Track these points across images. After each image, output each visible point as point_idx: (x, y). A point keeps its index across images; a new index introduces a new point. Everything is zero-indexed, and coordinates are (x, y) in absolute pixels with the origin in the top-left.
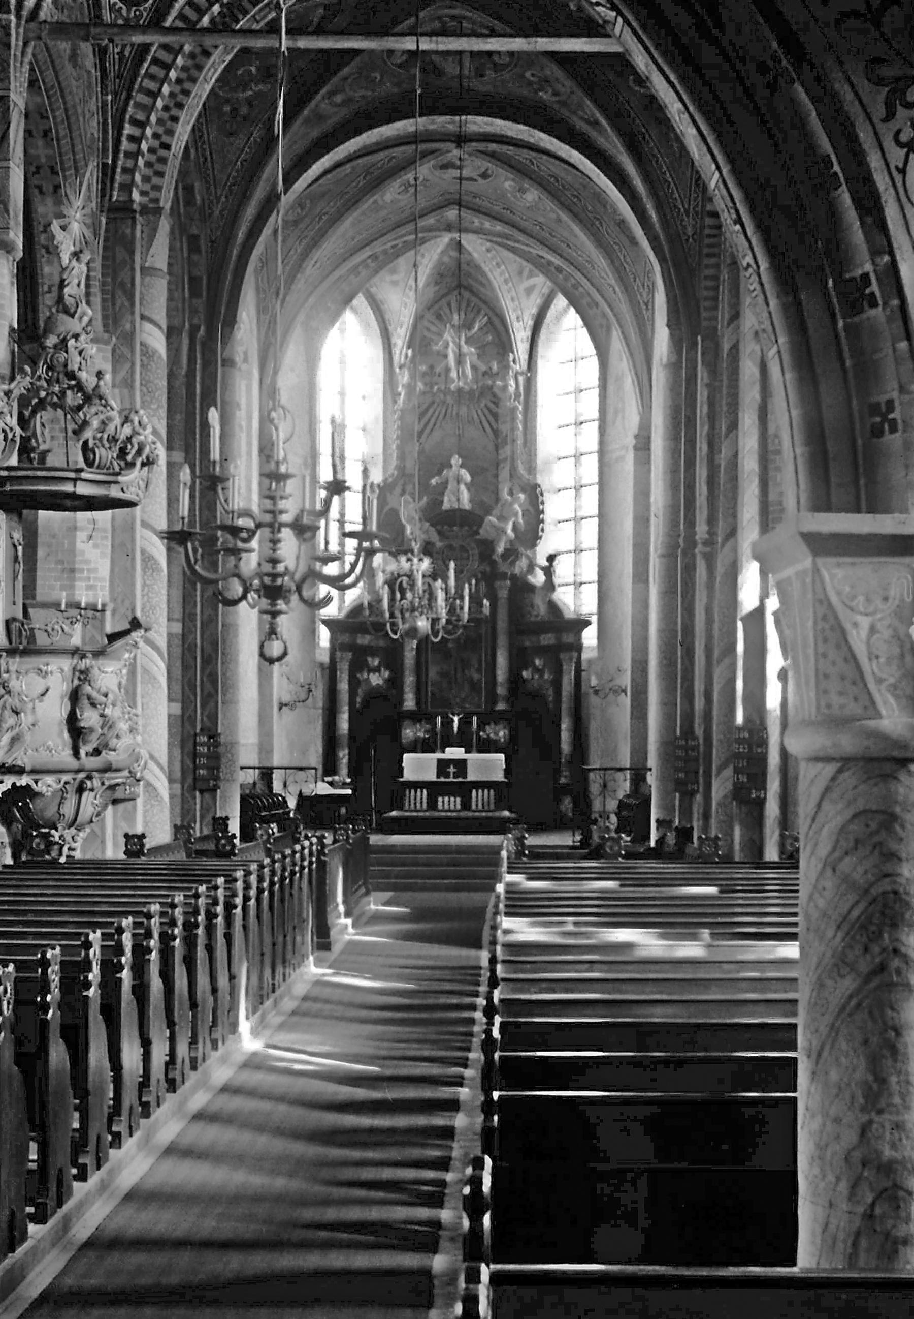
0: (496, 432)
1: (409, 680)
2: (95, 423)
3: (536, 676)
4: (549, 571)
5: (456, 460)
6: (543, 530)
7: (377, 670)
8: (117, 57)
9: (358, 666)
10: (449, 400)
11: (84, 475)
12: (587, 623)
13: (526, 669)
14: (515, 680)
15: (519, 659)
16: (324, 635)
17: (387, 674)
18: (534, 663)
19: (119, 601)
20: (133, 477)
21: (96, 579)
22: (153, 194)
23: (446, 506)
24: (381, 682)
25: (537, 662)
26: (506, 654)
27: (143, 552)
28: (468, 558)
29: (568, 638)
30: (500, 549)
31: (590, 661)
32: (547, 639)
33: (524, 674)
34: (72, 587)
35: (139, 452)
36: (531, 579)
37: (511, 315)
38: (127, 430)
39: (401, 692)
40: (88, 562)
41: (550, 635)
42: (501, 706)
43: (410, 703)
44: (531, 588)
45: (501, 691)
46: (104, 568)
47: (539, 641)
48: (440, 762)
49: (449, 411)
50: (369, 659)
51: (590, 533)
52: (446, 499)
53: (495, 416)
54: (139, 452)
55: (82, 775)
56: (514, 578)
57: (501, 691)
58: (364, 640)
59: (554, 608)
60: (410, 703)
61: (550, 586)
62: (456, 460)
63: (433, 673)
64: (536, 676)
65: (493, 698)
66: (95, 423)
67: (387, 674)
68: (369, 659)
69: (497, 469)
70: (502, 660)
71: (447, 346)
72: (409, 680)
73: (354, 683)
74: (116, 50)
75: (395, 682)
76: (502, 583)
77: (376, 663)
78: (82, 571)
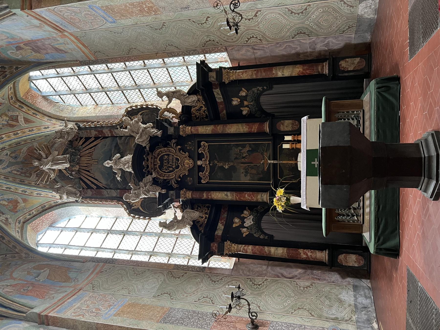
0: (96, 138)
1: (247, 197)
3: (246, 103)
4: (170, 96)
5: (108, 164)
6: (152, 105)
7: (243, 220)
10: (77, 168)
13: (242, 111)
18: (236, 106)
23: (130, 170)
24: (252, 217)
25: (235, 102)
26: (229, 126)
28: (168, 155)
30: (154, 131)
31: (232, 60)
33: (244, 113)
36: (179, 110)
37: (47, 132)
41: (215, 93)
42: (267, 129)
43: (264, 197)
44: (186, 109)
45: (255, 128)
47: (221, 102)
48: (308, 174)
49: (84, 168)
50: (234, 226)
52: (127, 170)
53: (87, 139)
56: (180, 123)
57: (255, 128)
59: (193, 91)
62: (108, 164)
63: (245, 179)
64: (246, 103)
65: (261, 134)
68: (234, 226)
69: (117, 137)
71: (54, 170)
72: (247, 197)
76: (181, 130)
77: (237, 220)
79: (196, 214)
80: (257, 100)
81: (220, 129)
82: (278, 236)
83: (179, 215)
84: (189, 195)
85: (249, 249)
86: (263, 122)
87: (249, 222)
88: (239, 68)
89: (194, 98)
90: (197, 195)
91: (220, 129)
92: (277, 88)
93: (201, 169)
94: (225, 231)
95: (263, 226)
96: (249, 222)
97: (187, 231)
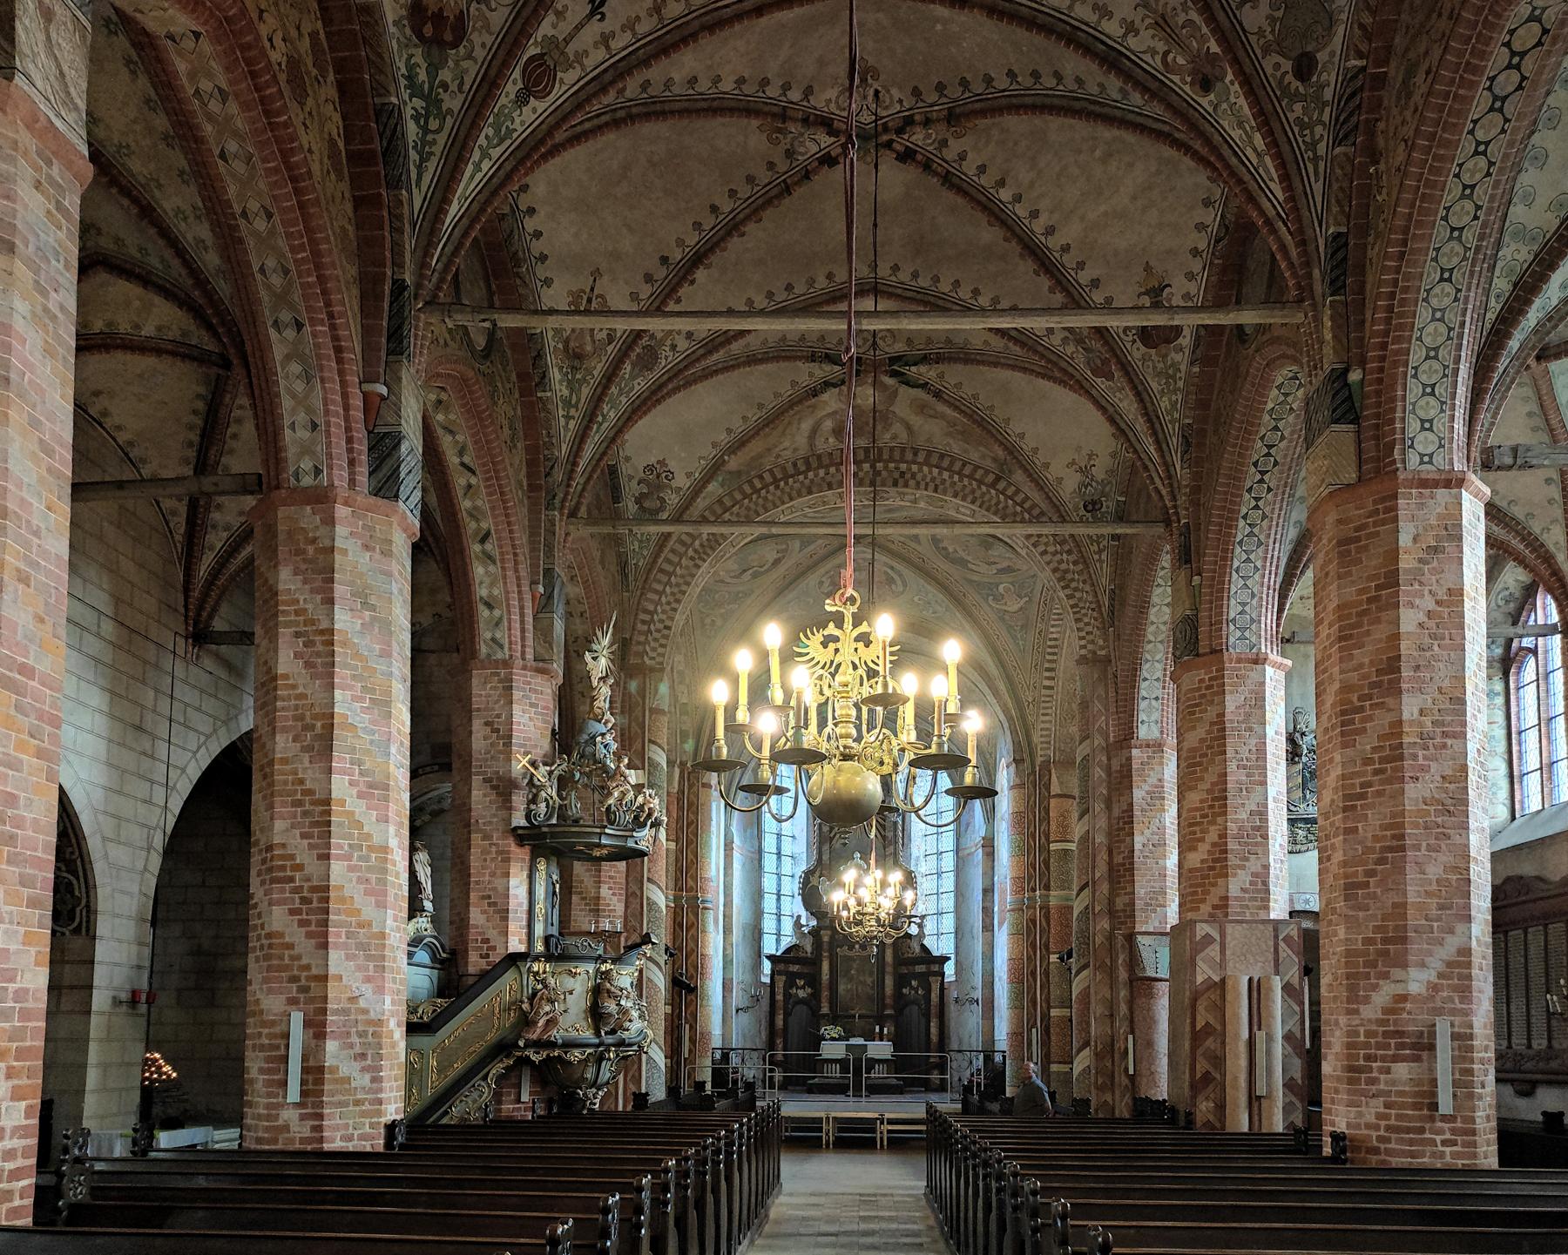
1: (825, 994)
2: (616, 794)
4: (920, 926)
7: (803, 987)
9: (790, 983)
12: (946, 959)
14: (898, 995)
15: (901, 981)
16: (767, 966)
17: (809, 990)
20: (645, 833)
29: (935, 968)
32: (921, 968)
35: (650, 815)
38: (640, 799)
39: (819, 1002)
42: (888, 1012)
43: (825, 1010)
51: (948, 902)
54: (650, 815)
58: (795, 968)
59: (923, 947)
60: (825, 1010)
61: (921, 935)
65: (884, 1007)
66: (616, 794)
67: (809, 990)
70: (889, 982)
72: (825, 994)
73: (787, 996)
75: (816, 996)
79: (809, 949)
80: (914, 1002)
81: (889, 969)
82: (790, 1019)
83: (806, 930)
84: (826, 939)
85: (780, 997)
86: (893, 1008)
87: (801, 994)
88: (942, 988)
89: (918, 949)
90: (825, 946)
91: (889, 969)
92: (923, 1020)
93: (851, 947)
94: (793, 973)
95: (798, 1007)
96: (801, 994)
97: (795, 941)
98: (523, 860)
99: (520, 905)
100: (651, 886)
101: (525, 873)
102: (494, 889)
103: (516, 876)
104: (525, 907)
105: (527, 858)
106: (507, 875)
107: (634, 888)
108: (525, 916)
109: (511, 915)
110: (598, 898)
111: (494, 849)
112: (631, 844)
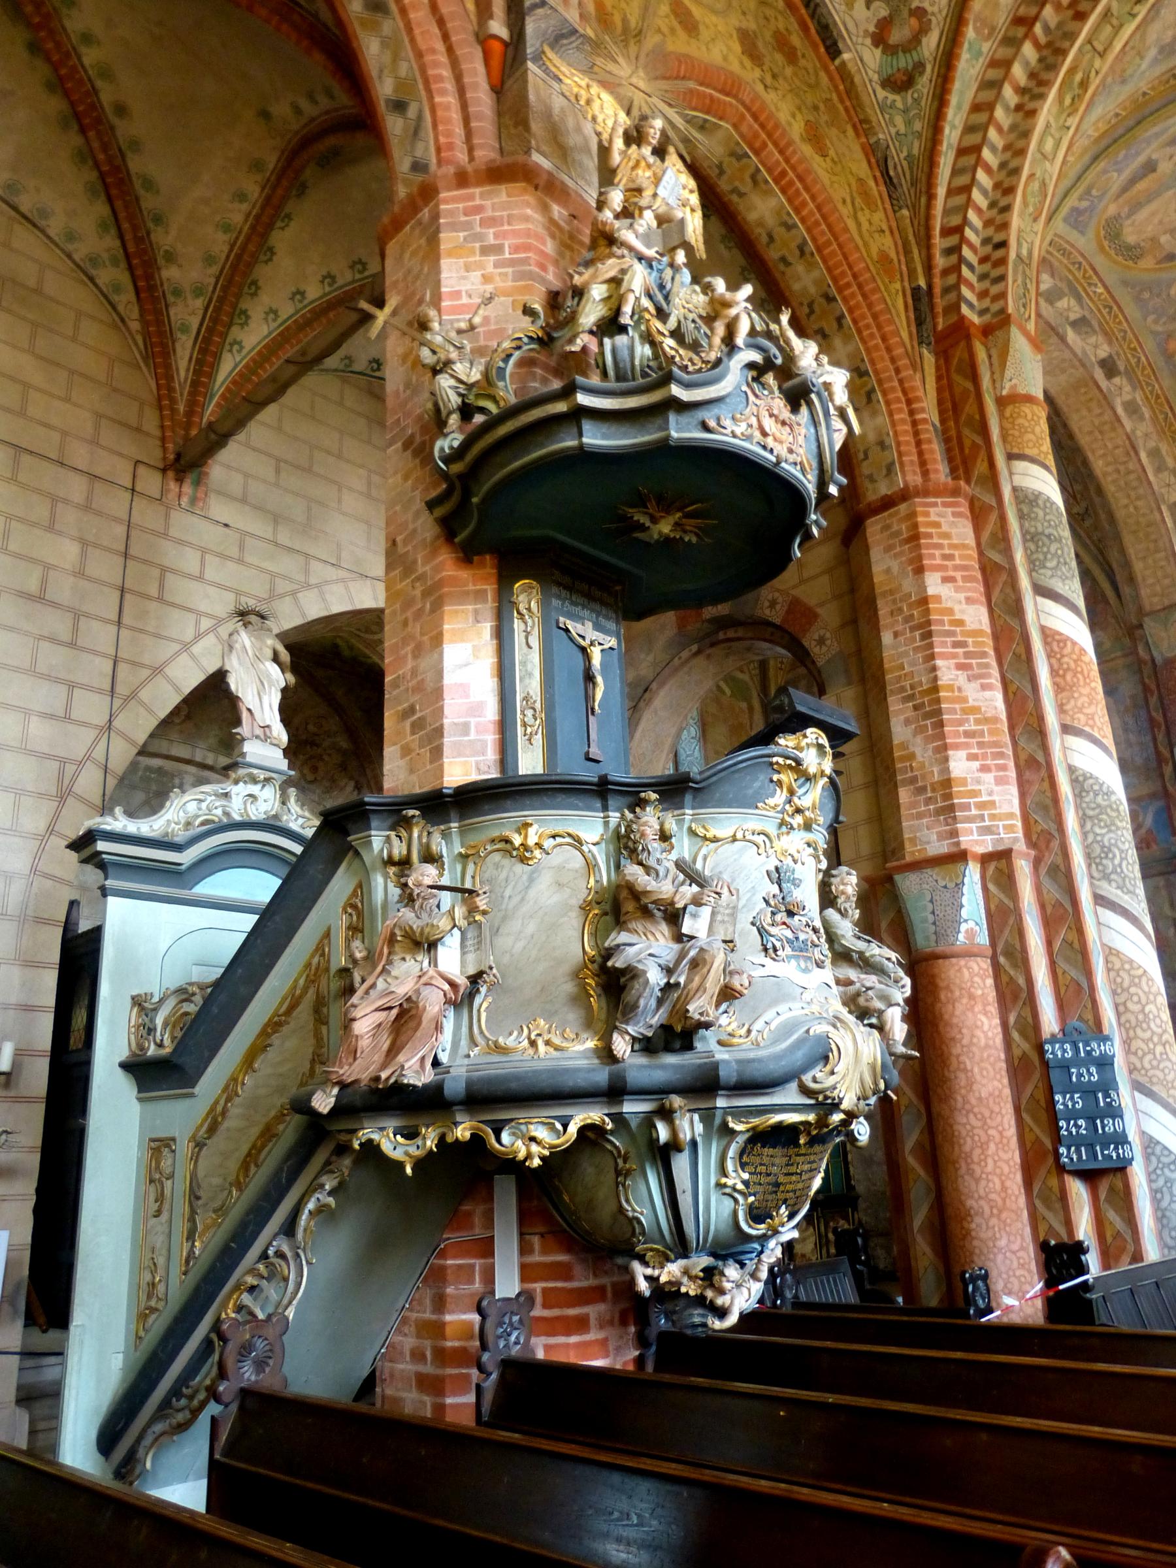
2: (598, 291)
8: (905, 163)
11: (583, 399)
19: (1042, 845)
21: (993, 817)
22: (995, 307)
27: (1071, 769)
34: (954, 833)
40: (975, 793)
46: (1008, 799)
55: (633, 1108)
74: (902, 156)
78: (967, 807)
98: (479, 596)
99: (476, 709)
100: (1073, 741)
101: (486, 628)
102: (419, 688)
103: (460, 636)
104: (491, 712)
105: (490, 589)
106: (437, 641)
107: (1030, 747)
108: (491, 739)
109: (447, 740)
110: (947, 783)
111: (418, 592)
112: (681, 430)
